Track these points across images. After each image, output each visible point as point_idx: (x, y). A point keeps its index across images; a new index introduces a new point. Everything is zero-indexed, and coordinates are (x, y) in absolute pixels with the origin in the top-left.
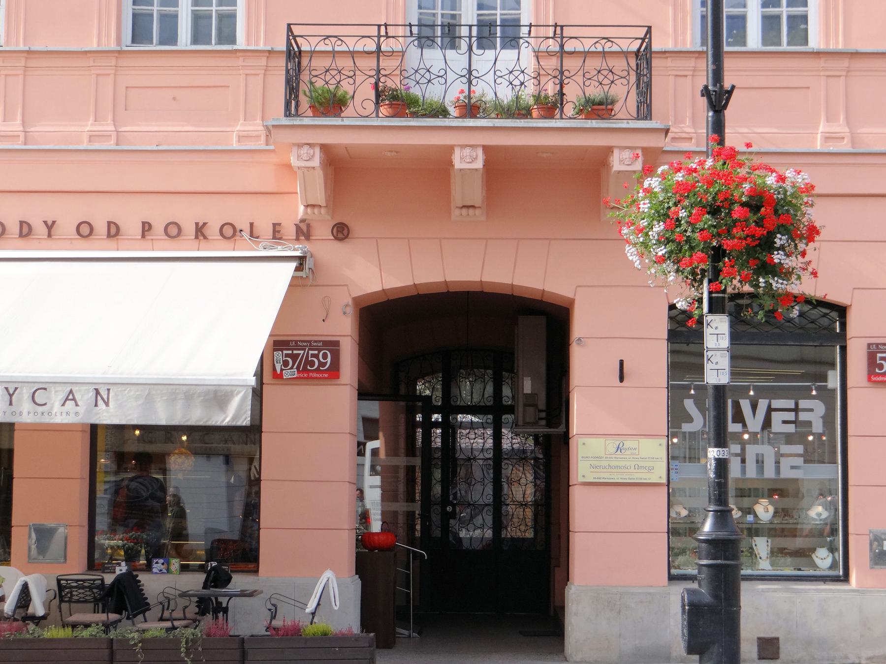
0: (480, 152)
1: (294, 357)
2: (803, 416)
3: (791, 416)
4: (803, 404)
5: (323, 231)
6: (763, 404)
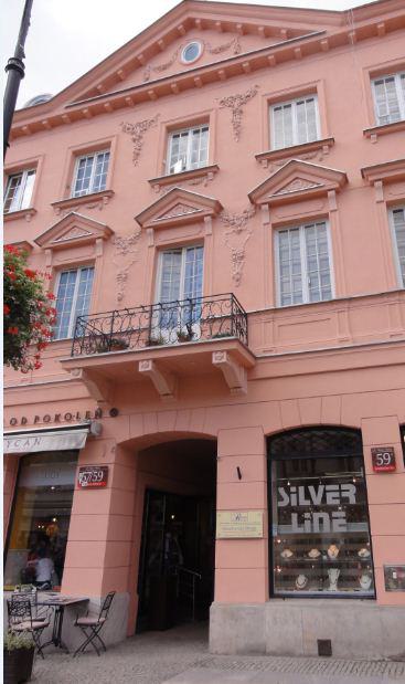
0: (150, 363)
1: (87, 475)
2: (344, 494)
3: (337, 494)
4: (344, 487)
5: (106, 414)
6: (321, 488)
